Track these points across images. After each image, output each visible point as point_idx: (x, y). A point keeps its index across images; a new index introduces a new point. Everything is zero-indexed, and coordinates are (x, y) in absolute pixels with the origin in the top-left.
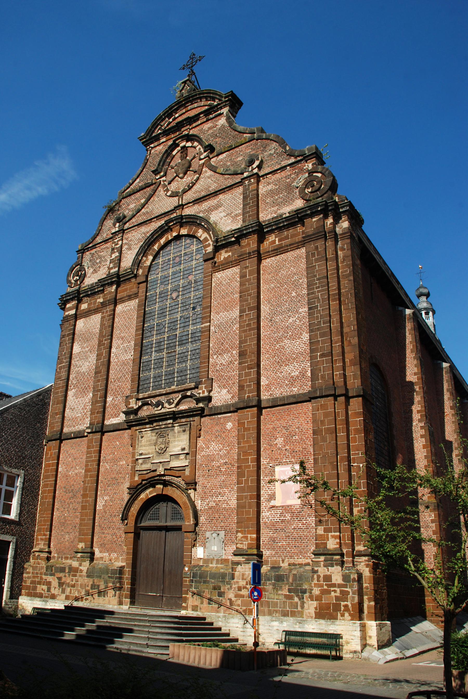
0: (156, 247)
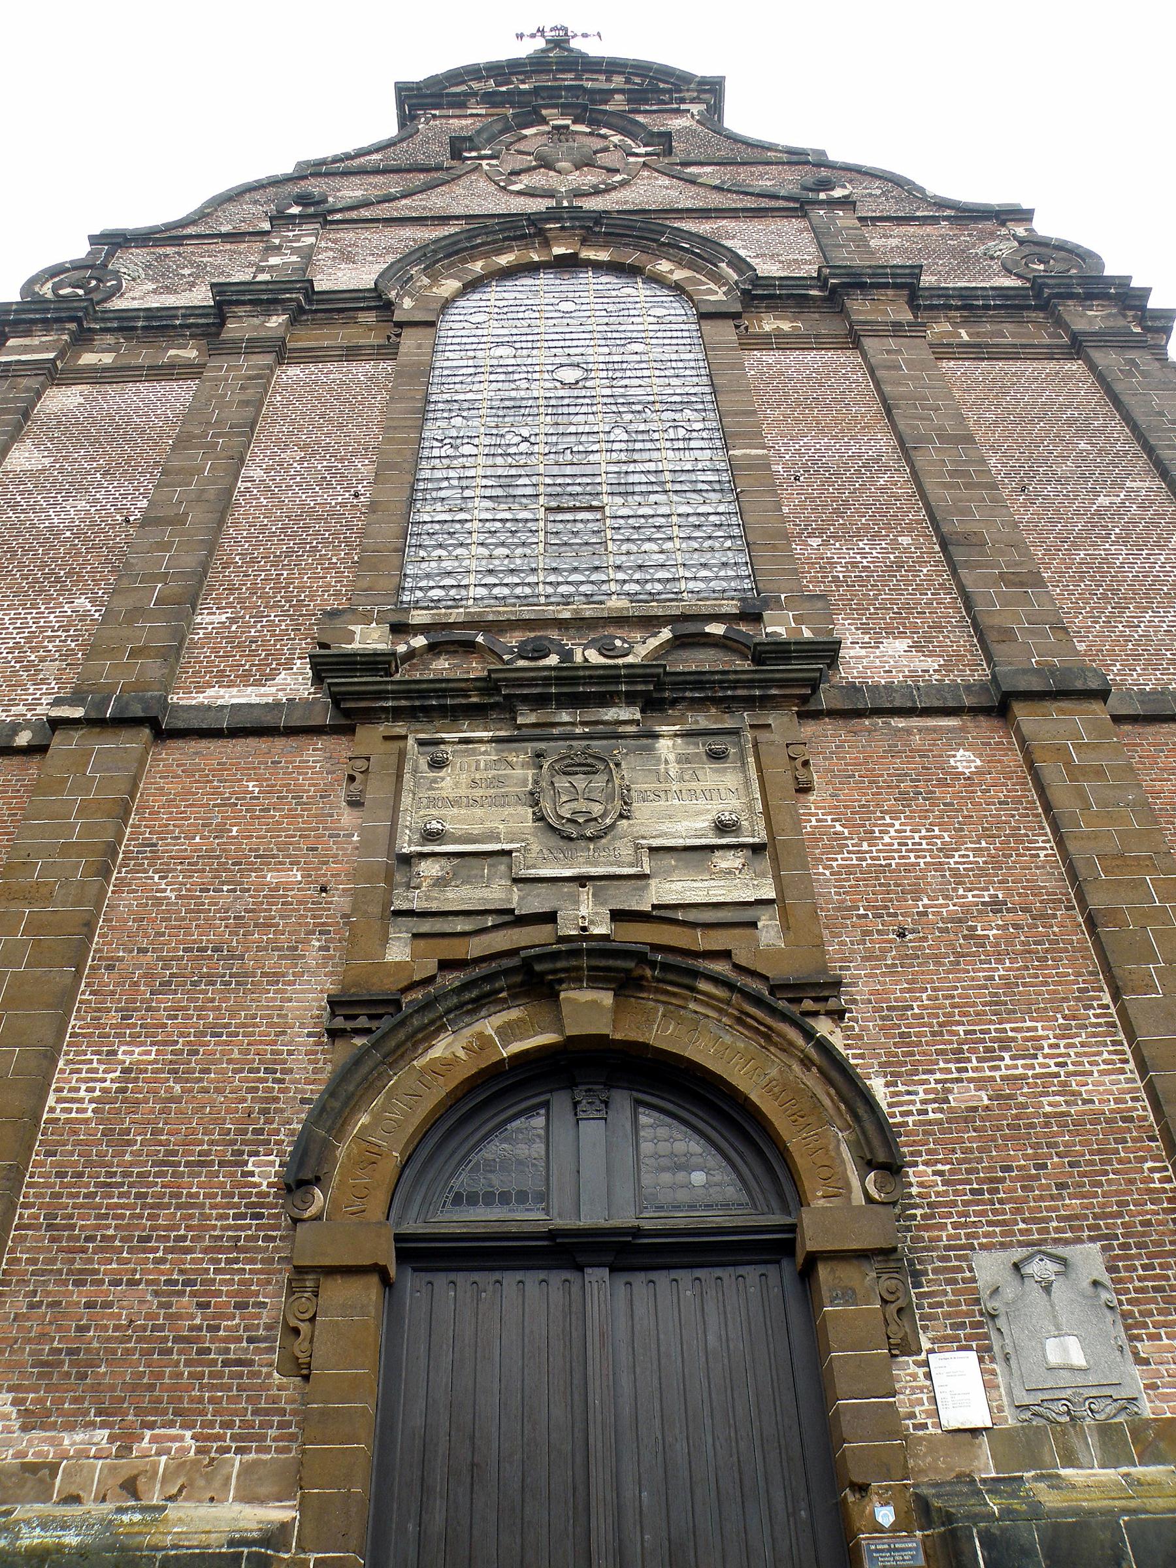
0: (478, 267)
